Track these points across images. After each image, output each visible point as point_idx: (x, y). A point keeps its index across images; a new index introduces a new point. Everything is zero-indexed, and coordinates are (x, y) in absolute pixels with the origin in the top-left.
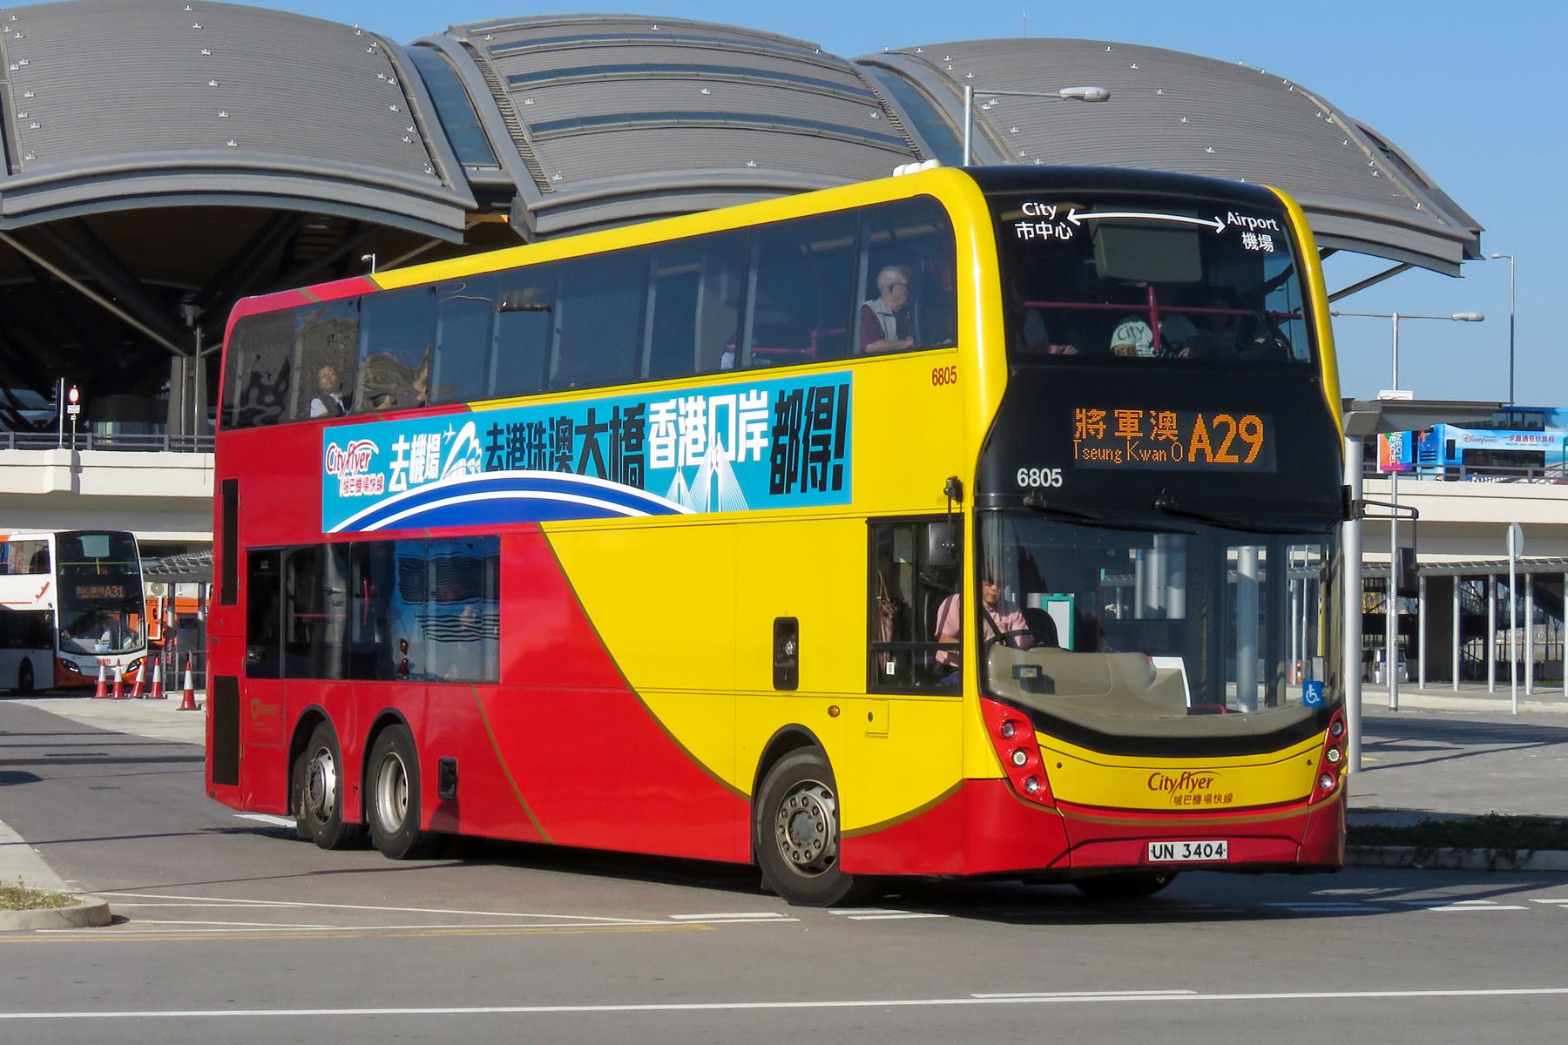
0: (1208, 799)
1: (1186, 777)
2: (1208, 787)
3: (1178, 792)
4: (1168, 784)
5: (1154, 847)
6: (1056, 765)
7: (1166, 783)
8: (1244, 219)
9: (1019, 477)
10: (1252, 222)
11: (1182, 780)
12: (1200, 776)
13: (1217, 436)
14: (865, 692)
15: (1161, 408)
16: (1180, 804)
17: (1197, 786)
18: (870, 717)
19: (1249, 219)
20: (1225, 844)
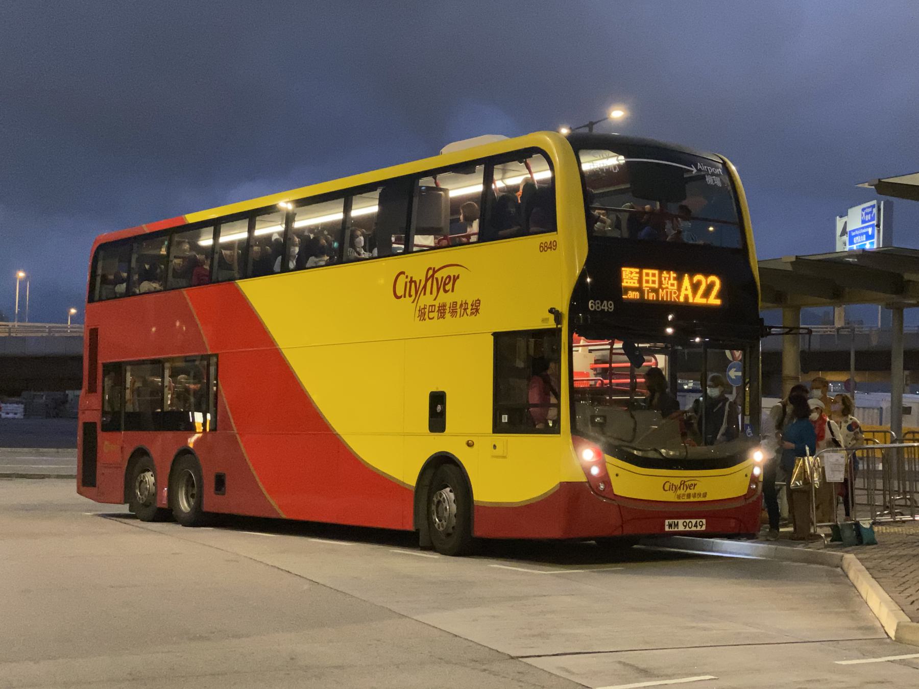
0: (694, 496)
1: (683, 483)
2: (694, 489)
3: (679, 492)
4: (674, 488)
5: (669, 522)
6: (615, 475)
7: (672, 488)
8: (705, 167)
9: (590, 305)
10: (710, 170)
11: (681, 485)
12: (690, 483)
13: (695, 287)
14: (492, 432)
15: (668, 270)
16: (680, 499)
17: (688, 489)
18: (495, 447)
19: (708, 168)
20: (704, 521)
